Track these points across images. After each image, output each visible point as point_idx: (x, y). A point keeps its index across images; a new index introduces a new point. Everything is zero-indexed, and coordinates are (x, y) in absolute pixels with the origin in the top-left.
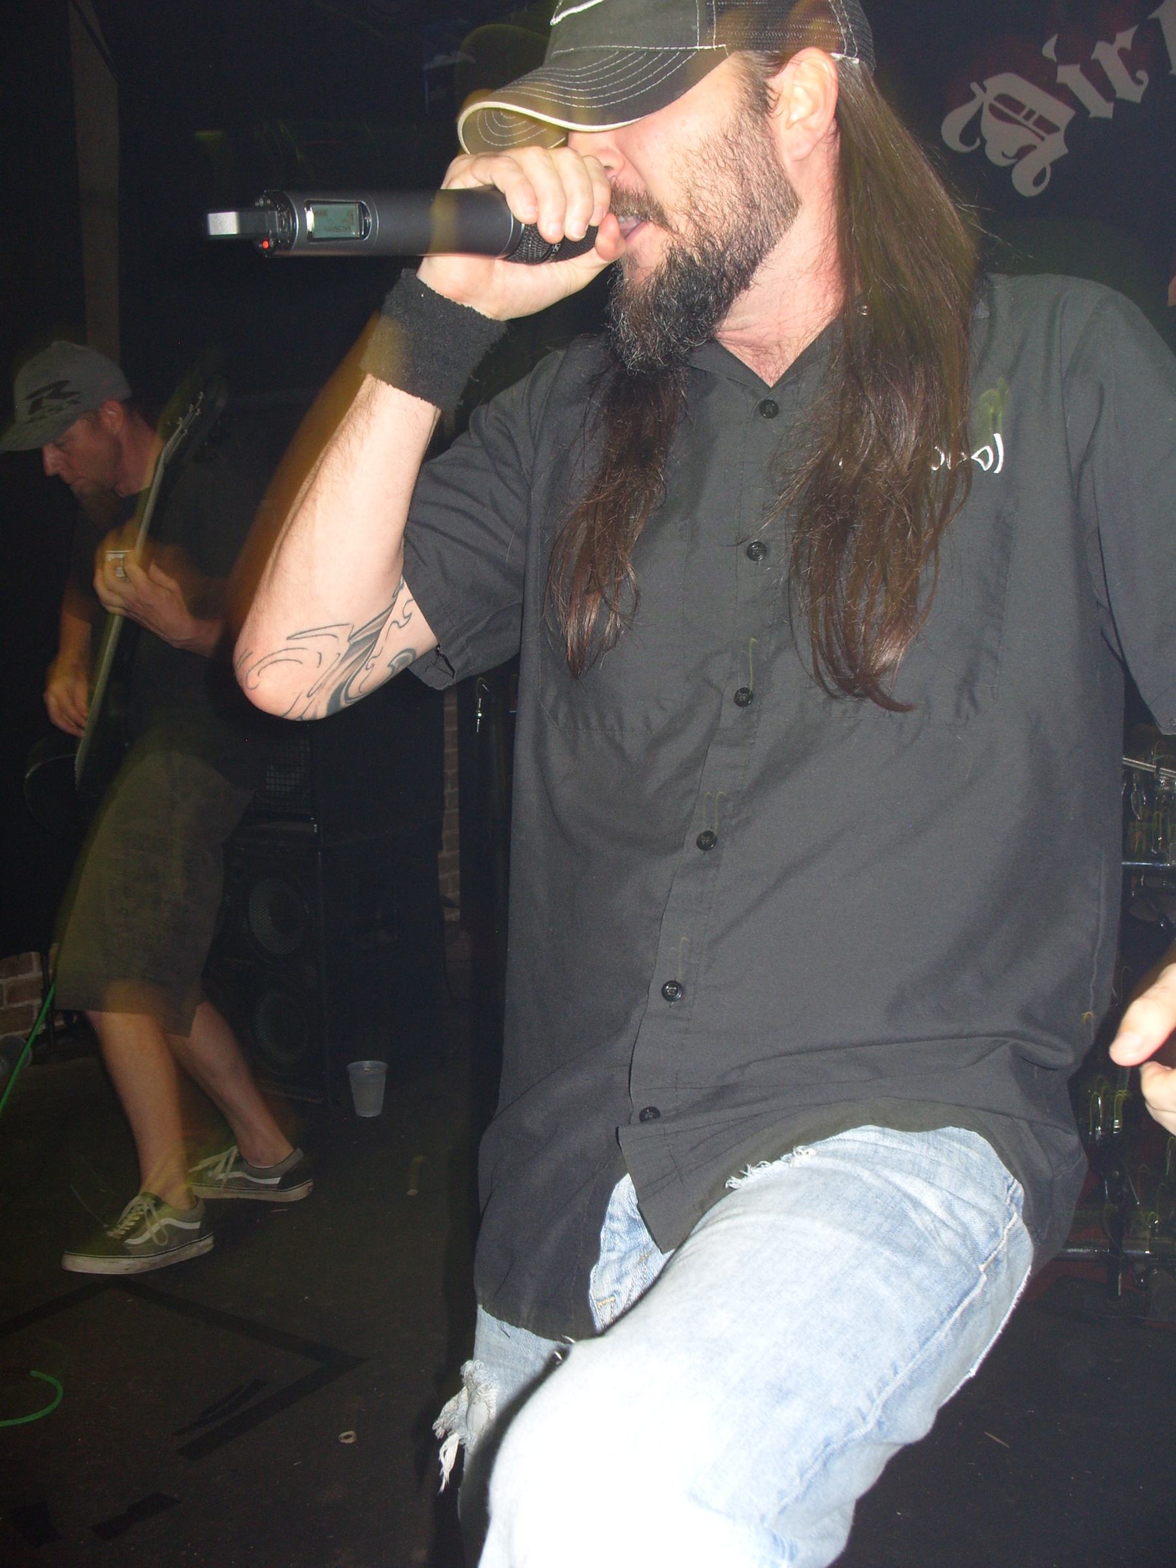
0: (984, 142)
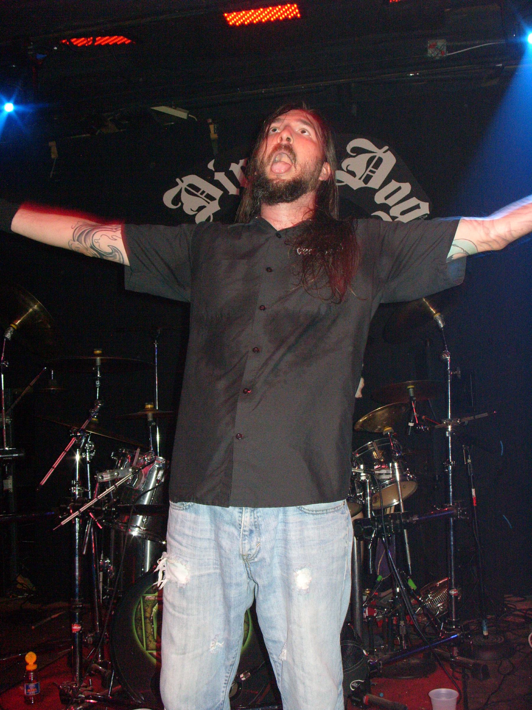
0: (182, 204)
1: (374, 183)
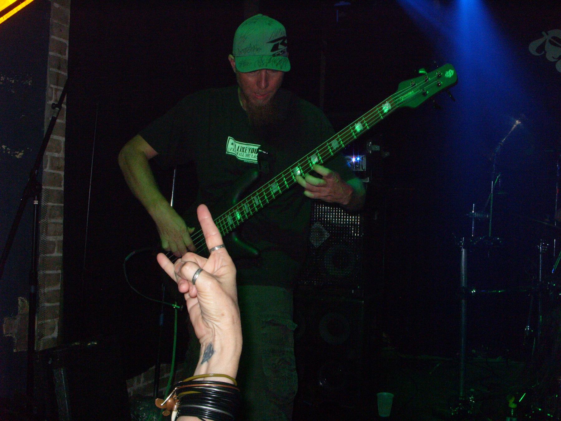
0: (546, 52)
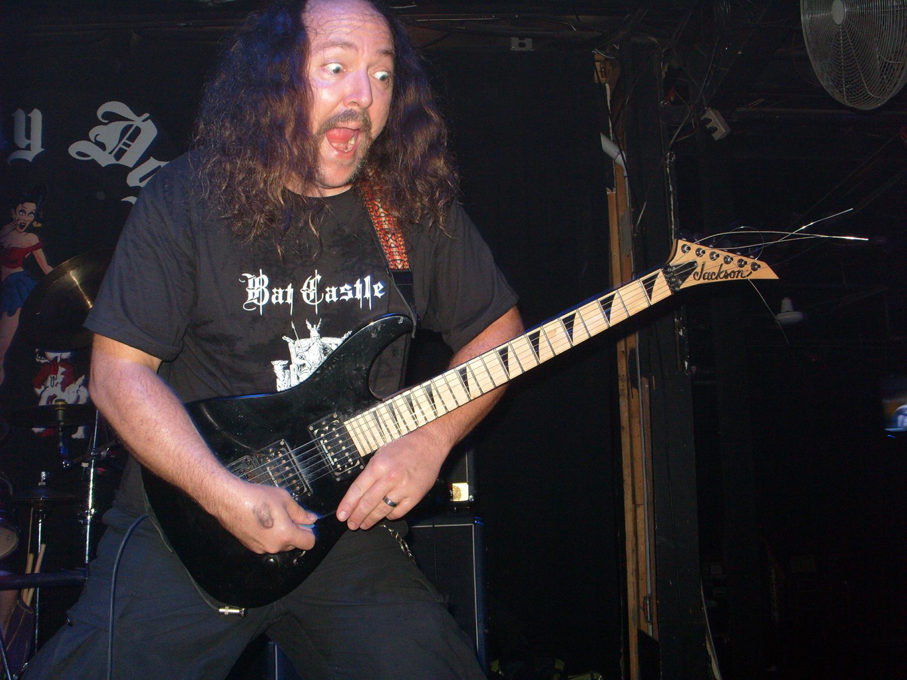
1: (128, 160)
